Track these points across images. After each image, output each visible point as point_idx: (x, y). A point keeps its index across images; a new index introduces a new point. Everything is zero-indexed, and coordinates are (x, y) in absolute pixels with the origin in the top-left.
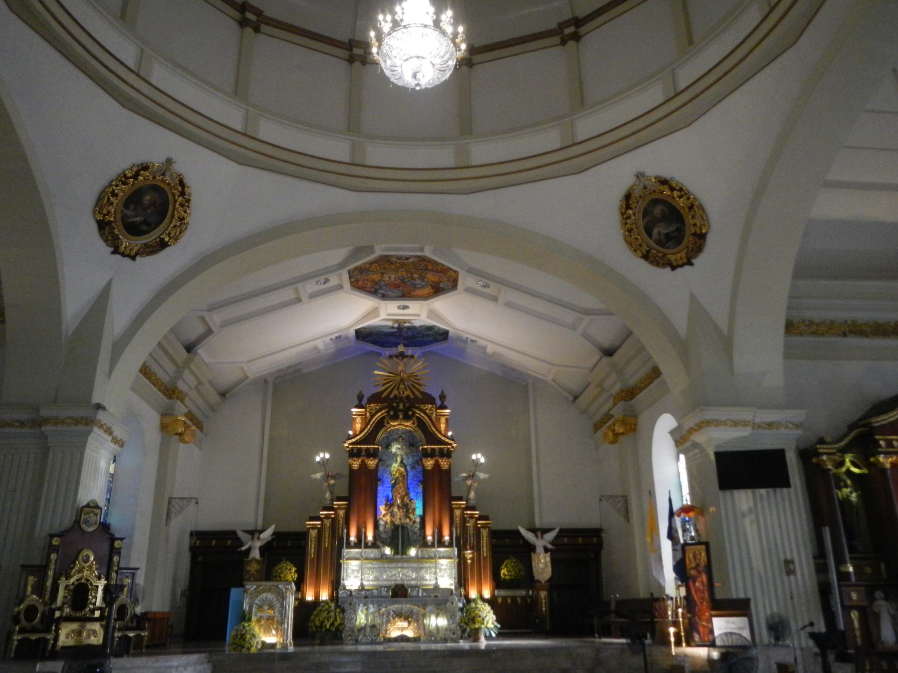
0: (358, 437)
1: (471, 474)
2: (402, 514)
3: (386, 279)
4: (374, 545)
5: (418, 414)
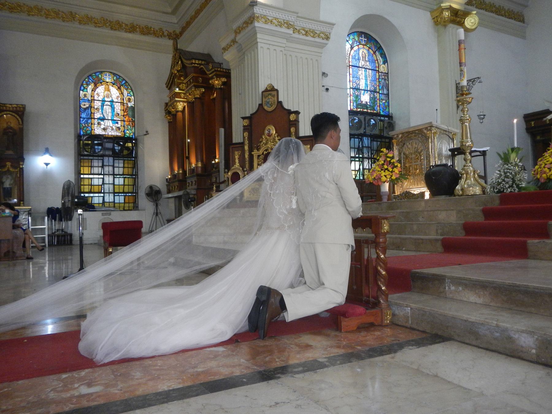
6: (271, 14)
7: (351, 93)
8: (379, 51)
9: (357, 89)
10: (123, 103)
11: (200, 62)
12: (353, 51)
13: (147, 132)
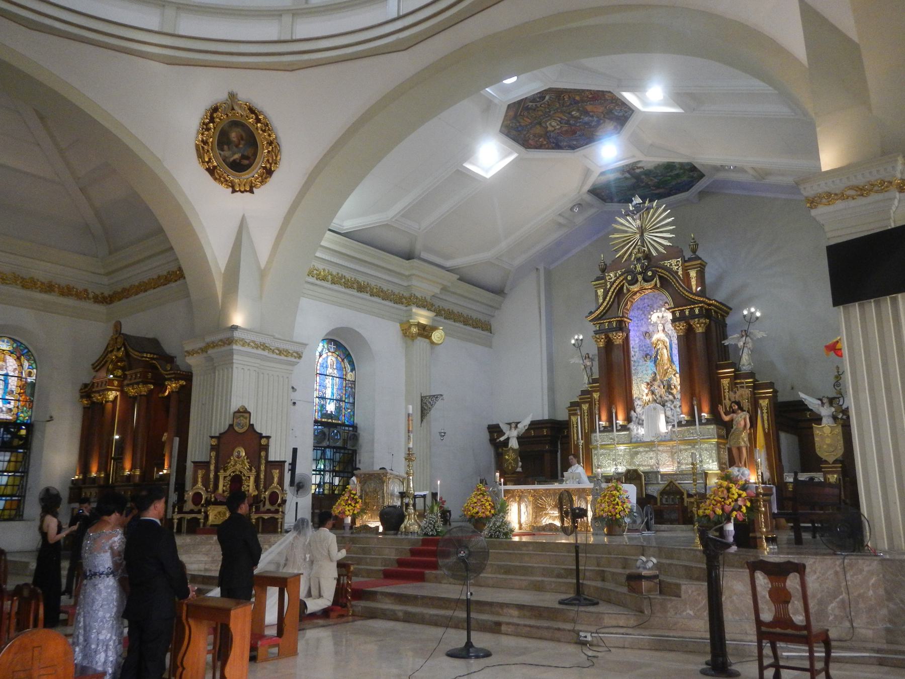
0: (598, 312)
1: (743, 334)
2: (664, 390)
3: (550, 128)
4: (624, 428)
5: (661, 273)
6: (248, 337)
7: (317, 402)
8: (347, 359)
9: (323, 398)
10: (21, 378)
11: (152, 356)
12: (321, 359)
13: (51, 417)
